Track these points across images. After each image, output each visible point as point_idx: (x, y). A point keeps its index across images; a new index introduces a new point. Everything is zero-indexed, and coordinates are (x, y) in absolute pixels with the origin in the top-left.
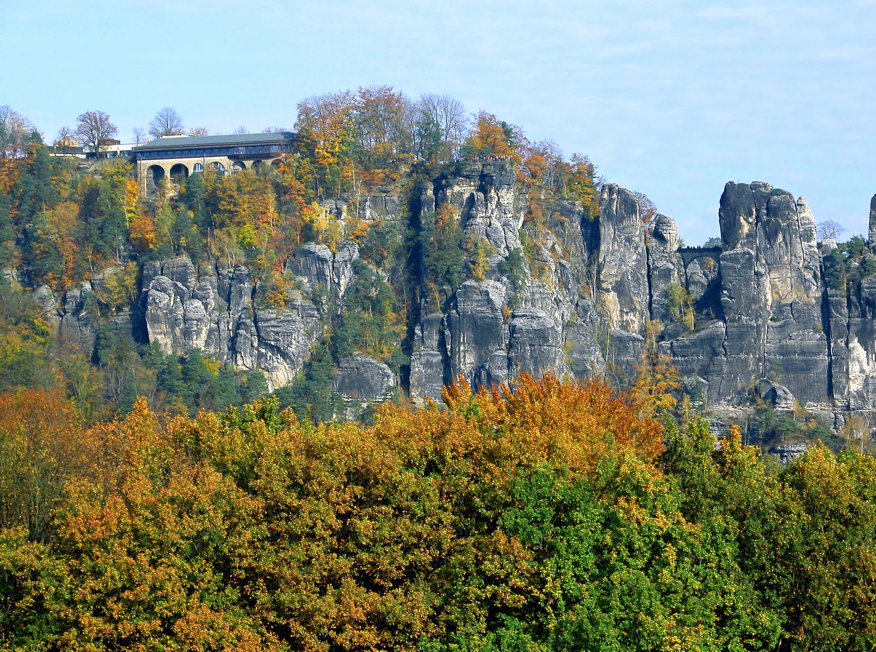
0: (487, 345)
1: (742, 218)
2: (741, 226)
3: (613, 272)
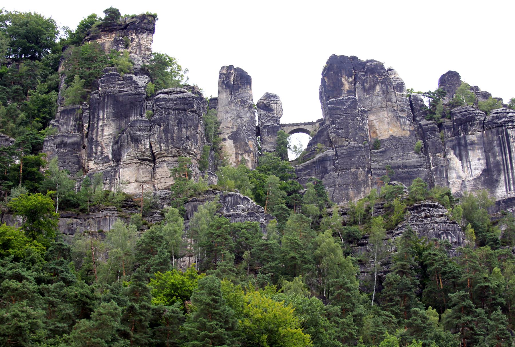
0: (127, 116)
1: (343, 79)
2: (342, 85)
3: (230, 125)
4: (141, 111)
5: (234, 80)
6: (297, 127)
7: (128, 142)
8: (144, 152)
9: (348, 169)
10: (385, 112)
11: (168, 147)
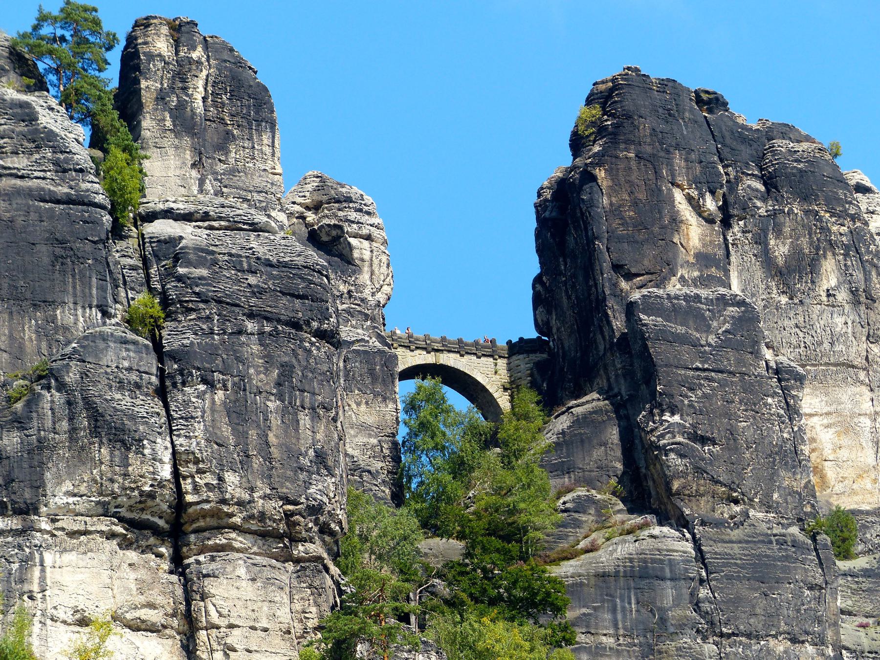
4: (102, 289)
5: (204, 99)
7: (73, 430)
8: (151, 495)
9: (758, 638)
10: (865, 390)
11: (252, 490)
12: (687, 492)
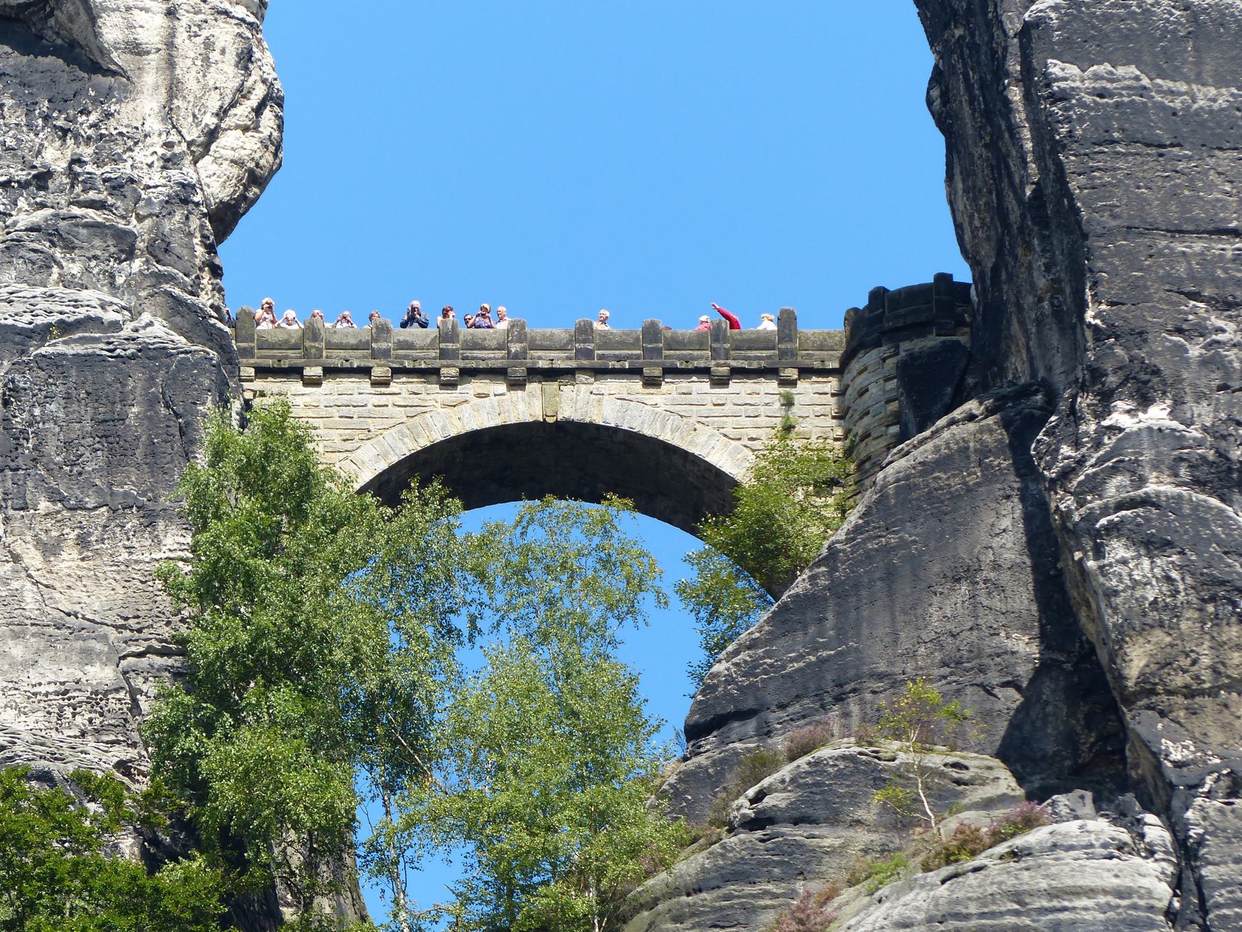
6: (523, 406)
12: (1179, 680)
